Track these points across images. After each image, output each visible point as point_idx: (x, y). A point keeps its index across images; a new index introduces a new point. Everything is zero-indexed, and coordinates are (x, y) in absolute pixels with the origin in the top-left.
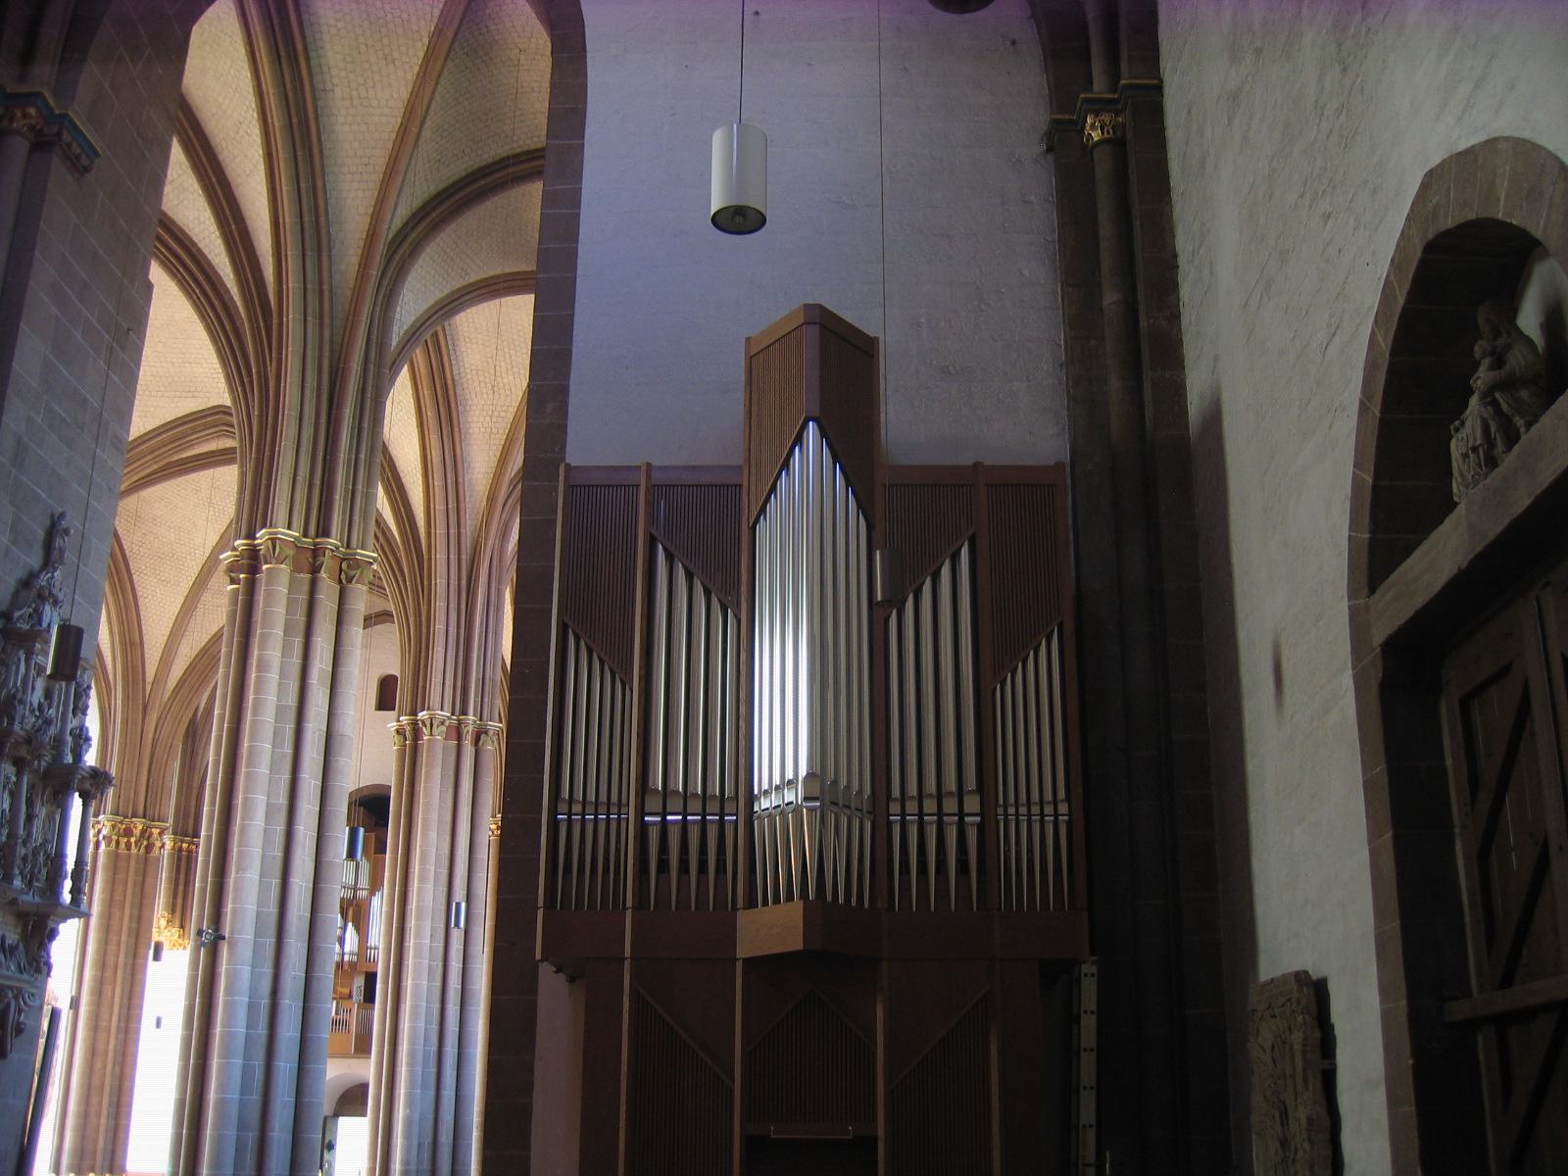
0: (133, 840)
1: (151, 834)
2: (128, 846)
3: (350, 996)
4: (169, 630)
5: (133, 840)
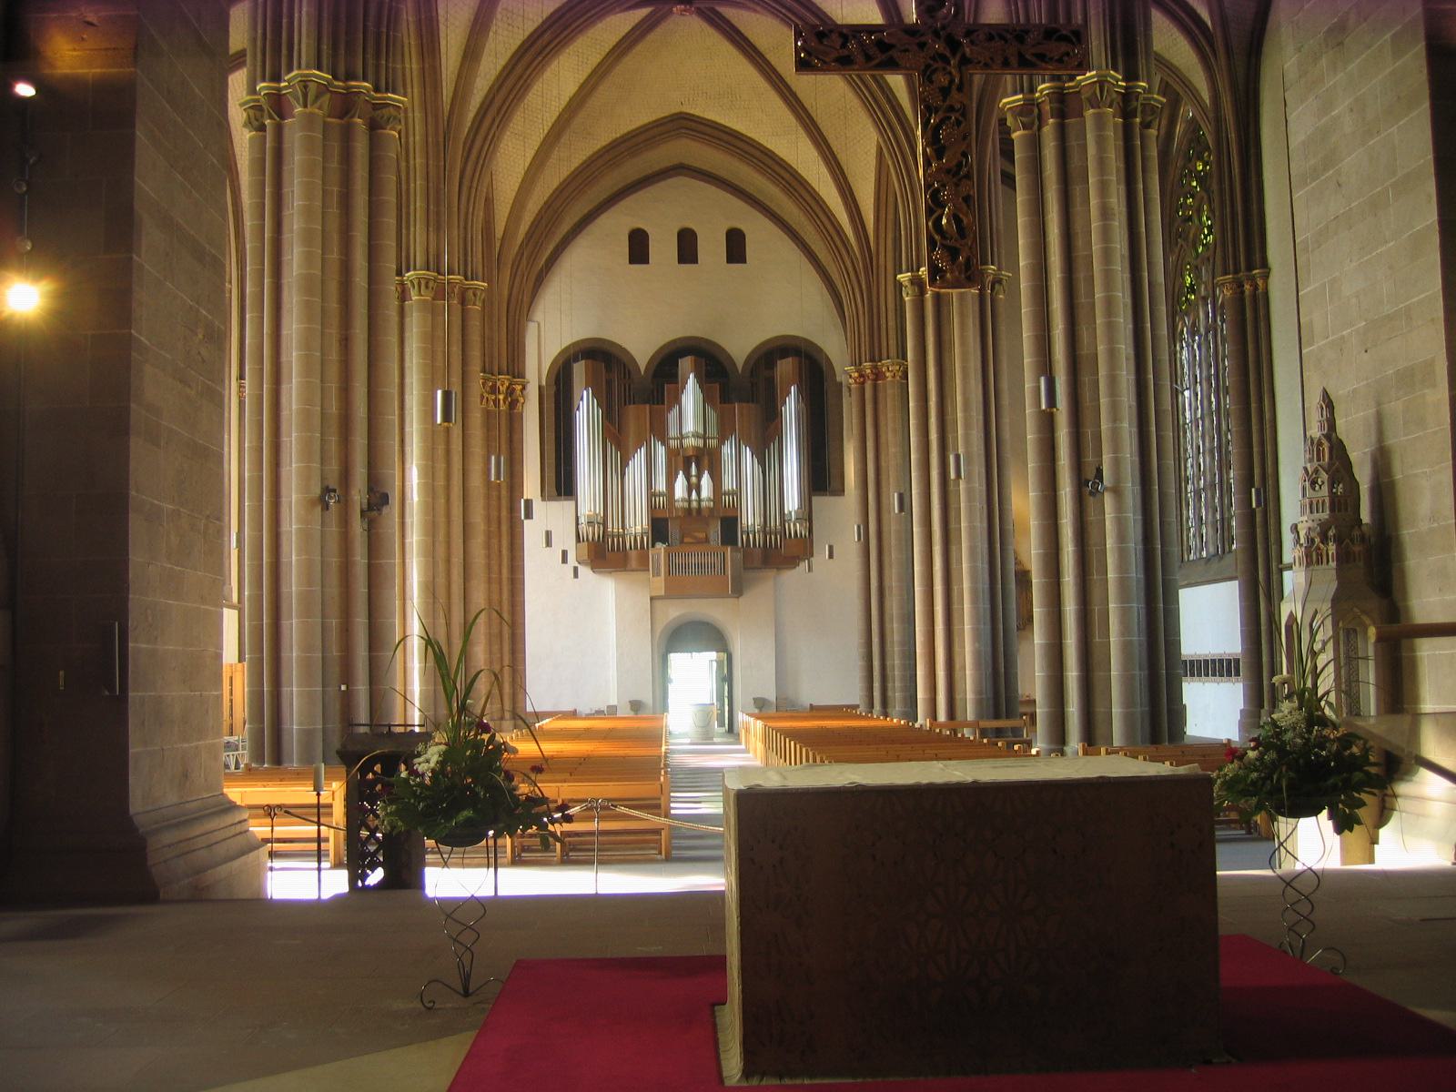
3: (707, 540)
4: (517, 185)
5: (501, 397)
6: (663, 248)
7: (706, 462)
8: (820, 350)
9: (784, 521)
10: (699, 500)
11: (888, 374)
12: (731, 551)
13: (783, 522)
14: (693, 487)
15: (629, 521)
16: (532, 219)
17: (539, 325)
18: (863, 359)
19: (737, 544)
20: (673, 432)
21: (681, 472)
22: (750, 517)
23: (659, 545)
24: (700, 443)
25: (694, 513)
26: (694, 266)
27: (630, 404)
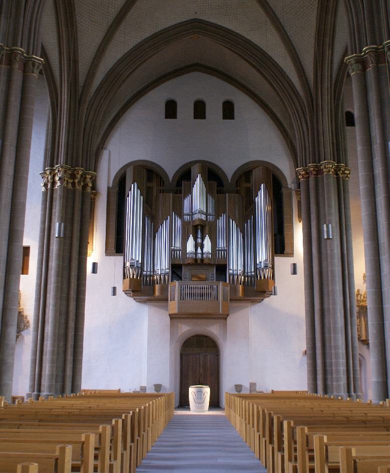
0: (76, 181)
1: (86, 178)
2: (73, 184)
5: (76, 181)
6: (185, 110)
7: (207, 228)
8: (278, 169)
9: (257, 268)
10: (202, 254)
11: (324, 170)
12: (223, 286)
13: (256, 269)
14: (199, 245)
15: (158, 268)
16: (103, 77)
17: (110, 151)
18: (308, 161)
19: (226, 282)
20: (186, 210)
21: (191, 236)
22: (236, 265)
23: (177, 283)
24: (204, 217)
25: (199, 262)
26: (203, 120)
27: (160, 193)
